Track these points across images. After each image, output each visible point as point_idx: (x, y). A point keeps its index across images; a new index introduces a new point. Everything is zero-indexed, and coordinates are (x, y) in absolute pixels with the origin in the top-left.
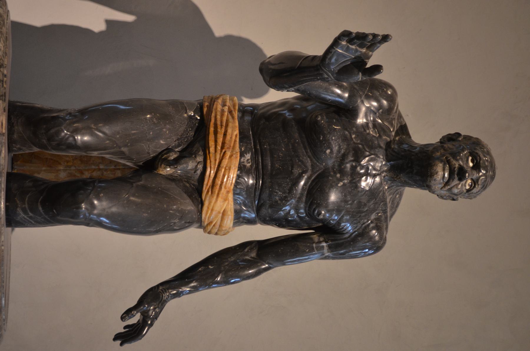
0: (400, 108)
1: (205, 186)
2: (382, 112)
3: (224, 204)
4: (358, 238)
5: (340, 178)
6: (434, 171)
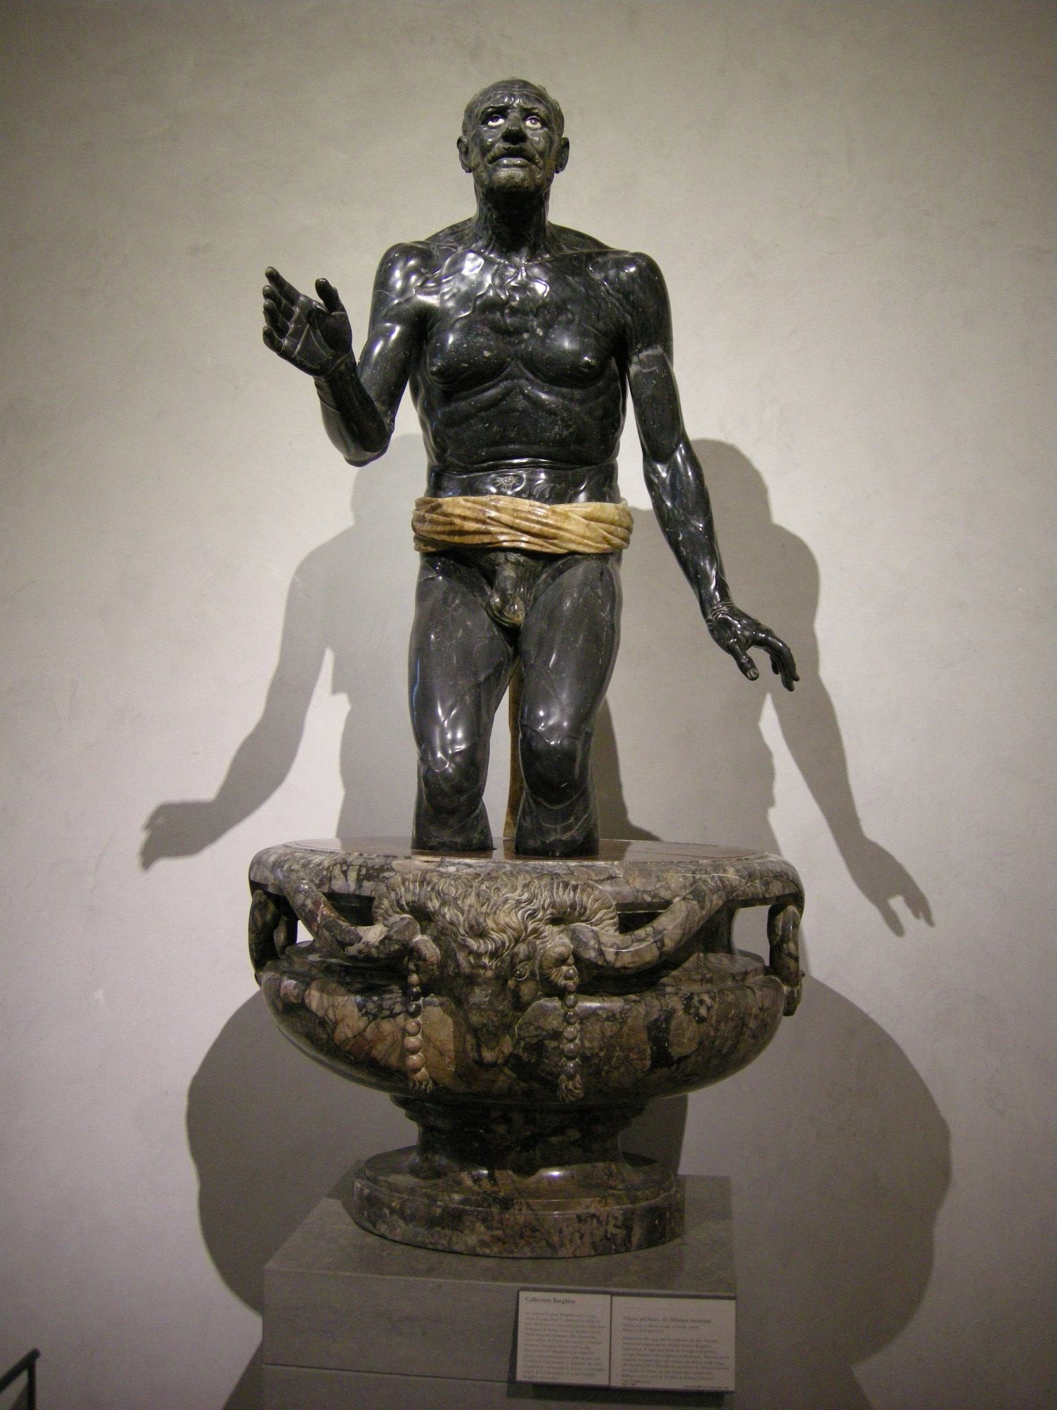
0: (423, 238)
1: (544, 550)
2: (425, 268)
3: (574, 519)
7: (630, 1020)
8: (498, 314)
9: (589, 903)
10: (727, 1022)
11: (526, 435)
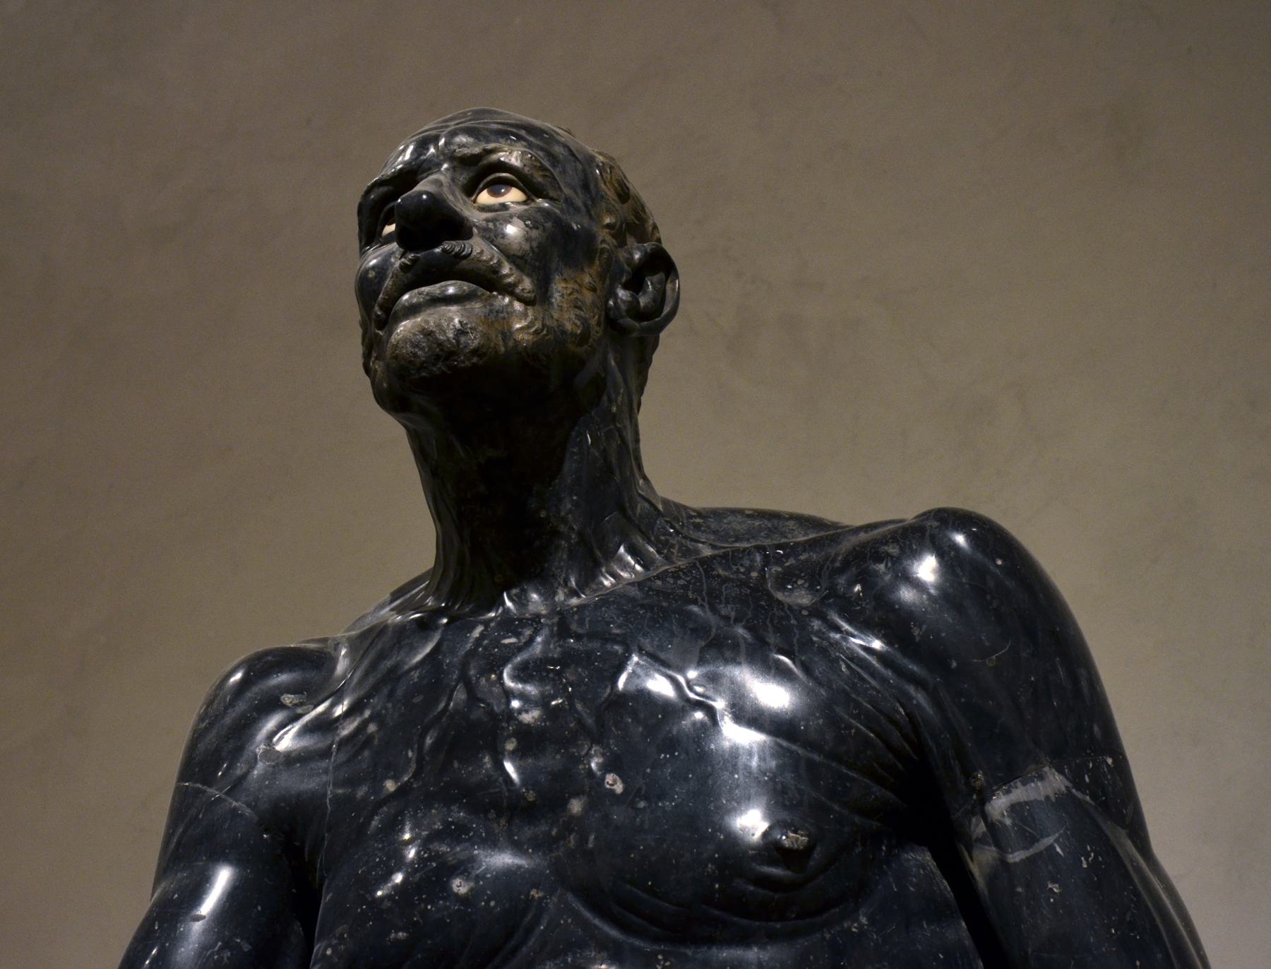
4: (917, 639)
5: (583, 793)
6: (422, 349)
8: (487, 759)
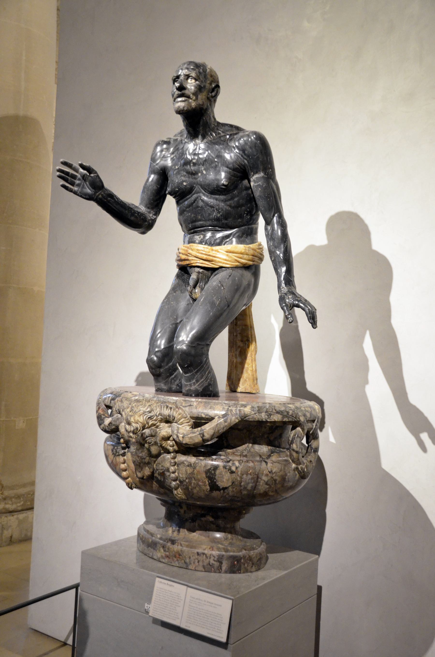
3: (221, 253)
7: (197, 468)
9: (176, 414)
10: (247, 475)
11: (204, 218)
